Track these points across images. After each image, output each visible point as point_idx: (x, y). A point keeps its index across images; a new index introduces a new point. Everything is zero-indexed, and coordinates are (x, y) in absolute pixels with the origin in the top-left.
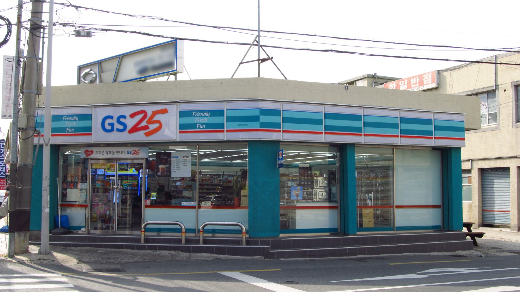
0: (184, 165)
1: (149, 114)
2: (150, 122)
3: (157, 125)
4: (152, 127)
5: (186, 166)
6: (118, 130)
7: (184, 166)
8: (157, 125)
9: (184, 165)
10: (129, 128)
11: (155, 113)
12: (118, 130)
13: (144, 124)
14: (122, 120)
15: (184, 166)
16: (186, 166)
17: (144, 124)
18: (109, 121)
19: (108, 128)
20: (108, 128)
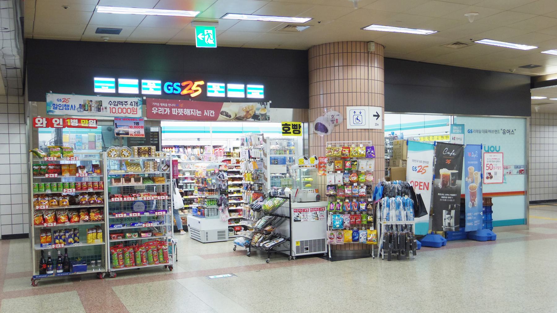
1: (423, 167)
2: (423, 170)
3: (425, 171)
8: (425, 171)
11: (424, 167)
13: (421, 170)
17: (421, 170)
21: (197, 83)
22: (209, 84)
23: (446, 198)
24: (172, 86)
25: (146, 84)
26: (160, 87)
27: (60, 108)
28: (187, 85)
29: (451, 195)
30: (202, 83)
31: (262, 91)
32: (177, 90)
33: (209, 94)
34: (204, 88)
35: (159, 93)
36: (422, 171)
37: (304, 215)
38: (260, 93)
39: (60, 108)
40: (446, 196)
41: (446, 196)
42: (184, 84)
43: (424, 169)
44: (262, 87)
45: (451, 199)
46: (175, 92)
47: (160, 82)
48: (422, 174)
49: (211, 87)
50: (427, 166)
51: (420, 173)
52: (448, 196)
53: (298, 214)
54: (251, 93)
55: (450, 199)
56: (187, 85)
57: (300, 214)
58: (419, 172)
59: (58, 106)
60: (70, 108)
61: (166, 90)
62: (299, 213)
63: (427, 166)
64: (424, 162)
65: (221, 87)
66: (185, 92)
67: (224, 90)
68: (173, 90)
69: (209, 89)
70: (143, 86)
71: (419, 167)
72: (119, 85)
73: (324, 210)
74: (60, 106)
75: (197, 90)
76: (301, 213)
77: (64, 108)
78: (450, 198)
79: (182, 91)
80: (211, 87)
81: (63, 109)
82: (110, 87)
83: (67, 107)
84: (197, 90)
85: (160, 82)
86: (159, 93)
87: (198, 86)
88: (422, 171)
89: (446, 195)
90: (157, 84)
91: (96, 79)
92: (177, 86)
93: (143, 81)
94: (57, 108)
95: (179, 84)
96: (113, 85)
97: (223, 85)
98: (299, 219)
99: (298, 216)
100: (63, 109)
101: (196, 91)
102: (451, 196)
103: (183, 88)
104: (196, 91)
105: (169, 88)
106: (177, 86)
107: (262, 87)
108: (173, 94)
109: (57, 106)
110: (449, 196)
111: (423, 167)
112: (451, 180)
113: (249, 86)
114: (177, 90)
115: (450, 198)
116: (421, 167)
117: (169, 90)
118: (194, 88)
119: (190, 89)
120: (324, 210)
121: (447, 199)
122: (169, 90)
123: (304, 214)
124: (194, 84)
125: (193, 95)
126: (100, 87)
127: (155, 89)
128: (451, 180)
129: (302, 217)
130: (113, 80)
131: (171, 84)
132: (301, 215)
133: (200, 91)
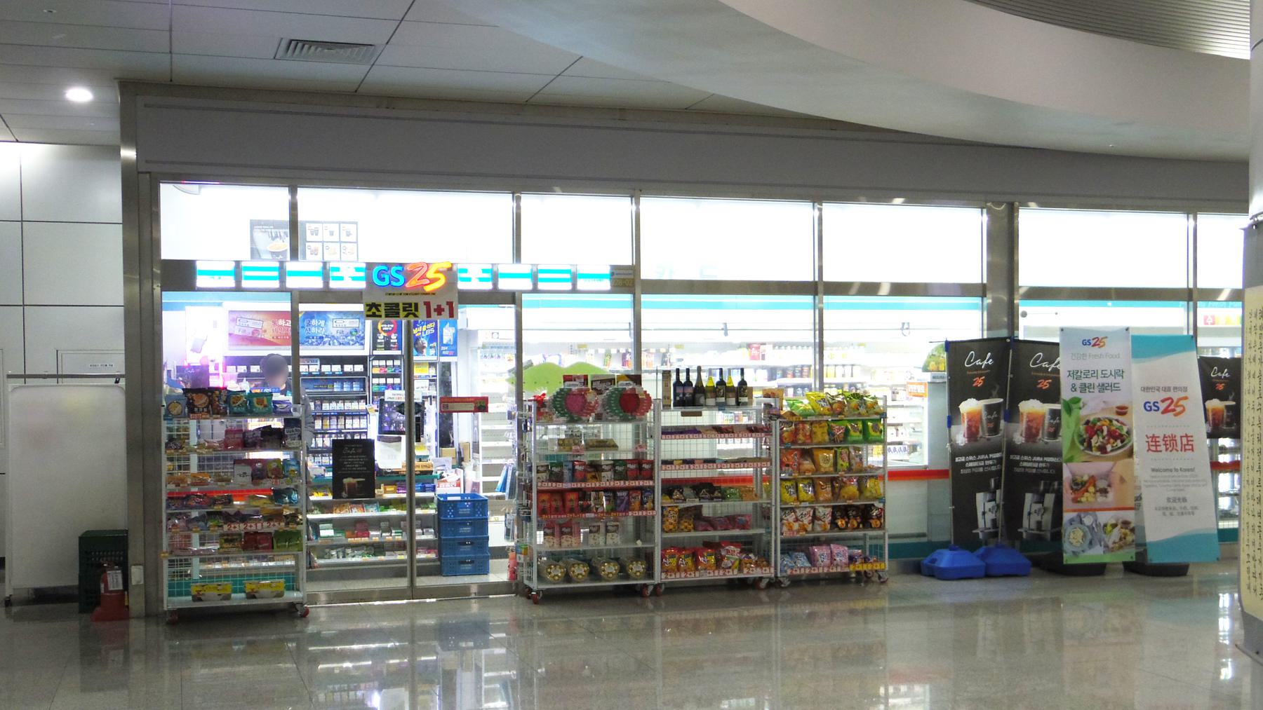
1: (1175, 401)
2: (1177, 406)
4: (1179, 409)
10: (1162, 409)
13: (1172, 407)
17: (1172, 407)
29: (991, 456)
36: (1174, 410)
41: (980, 460)
48: (1176, 415)
52: (984, 460)
55: (990, 466)
78: (991, 462)
88: (1174, 410)
101: (432, 281)
102: (991, 459)
104: (432, 281)
110: (987, 460)
111: (1175, 401)
115: (991, 462)
119: (423, 277)
121: (984, 466)
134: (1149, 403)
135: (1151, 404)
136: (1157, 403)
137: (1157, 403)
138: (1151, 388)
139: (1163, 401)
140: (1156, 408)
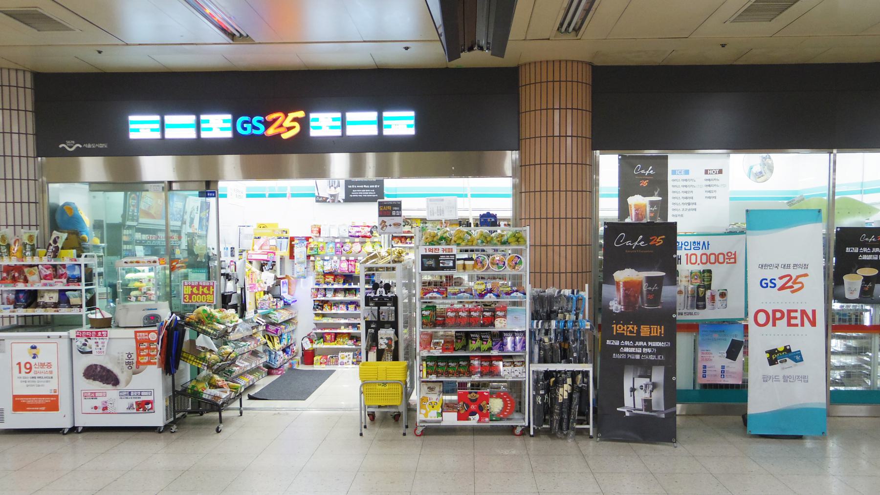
0: (709, 195)
1: (794, 277)
2: (794, 282)
3: (800, 285)
4: (796, 286)
5: (715, 197)
6: (771, 287)
7: (710, 198)
8: (800, 285)
9: (709, 195)
10: (778, 286)
11: (798, 277)
12: (771, 287)
13: (790, 284)
14: (773, 281)
15: (710, 198)
16: (715, 197)
17: (790, 284)
18: (764, 282)
19: (765, 285)
20: (765, 285)
21: (292, 115)
22: (312, 116)
23: (639, 350)
24: (250, 122)
25: (208, 121)
26: (229, 125)
27: (687, 248)
28: (275, 120)
29: (650, 343)
30: (301, 114)
31: (412, 122)
32: (258, 129)
33: (313, 133)
34: (304, 123)
35: (229, 134)
36: (791, 287)
37: (97, 343)
38: (409, 126)
39: (687, 248)
40: (637, 347)
41: (637, 347)
42: (270, 117)
43: (799, 280)
44: (412, 114)
45: (651, 354)
46: (255, 132)
47: (229, 117)
48: (793, 292)
49: (317, 120)
50: (806, 275)
51: (789, 290)
52: (642, 347)
53: (86, 341)
54: (389, 126)
55: (648, 354)
56: (275, 120)
57: (88, 340)
58: (783, 288)
59: (683, 246)
60: (701, 247)
61: (240, 130)
62: (86, 338)
63: (806, 275)
64: (795, 265)
65: (334, 119)
66: (271, 131)
67: (339, 123)
68: (252, 130)
69: (312, 124)
70: (203, 126)
71: (781, 278)
72: (165, 126)
73: (105, 335)
74: (686, 244)
75: (294, 127)
76: (90, 339)
77: (693, 247)
78: (649, 350)
79: (266, 128)
80: (317, 120)
81: (691, 249)
82: (153, 130)
83: (696, 246)
84: (294, 127)
85: (229, 117)
86: (229, 134)
87: (295, 120)
88: (791, 287)
89: (637, 344)
90: (225, 121)
91: (131, 118)
92: (259, 121)
93: (203, 117)
94: (681, 247)
95: (261, 118)
96: (158, 126)
97: (338, 115)
98: (88, 349)
99: (85, 345)
100: (691, 249)
101: (289, 129)
102: (650, 347)
103: (268, 125)
104: (289, 129)
105: (245, 125)
106: (259, 121)
107: (412, 114)
108: (252, 135)
109: (682, 244)
110: (645, 347)
111: (794, 277)
112: (645, 292)
113: (386, 114)
114: (258, 129)
115: (649, 350)
116: (788, 278)
117: (245, 129)
118: (287, 123)
119: (281, 126)
120: (105, 335)
121: (641, 354)
122: (245, 129)
123: (98, 340)
124: (286, 116)
125: (285, 136)
126: (137, 130)
127: (222, 129)
128: (645, 292)
129: (94, 346)
130: (157, 118)
131: (247, 118)
132: (91, 342)
133: (297, 129)
134: (766, 280)
135: (768, 281)
136: (775, 279)
137: (775, 279)
138: (770, 265)
139: (781, 278)
140: (773, 285)
